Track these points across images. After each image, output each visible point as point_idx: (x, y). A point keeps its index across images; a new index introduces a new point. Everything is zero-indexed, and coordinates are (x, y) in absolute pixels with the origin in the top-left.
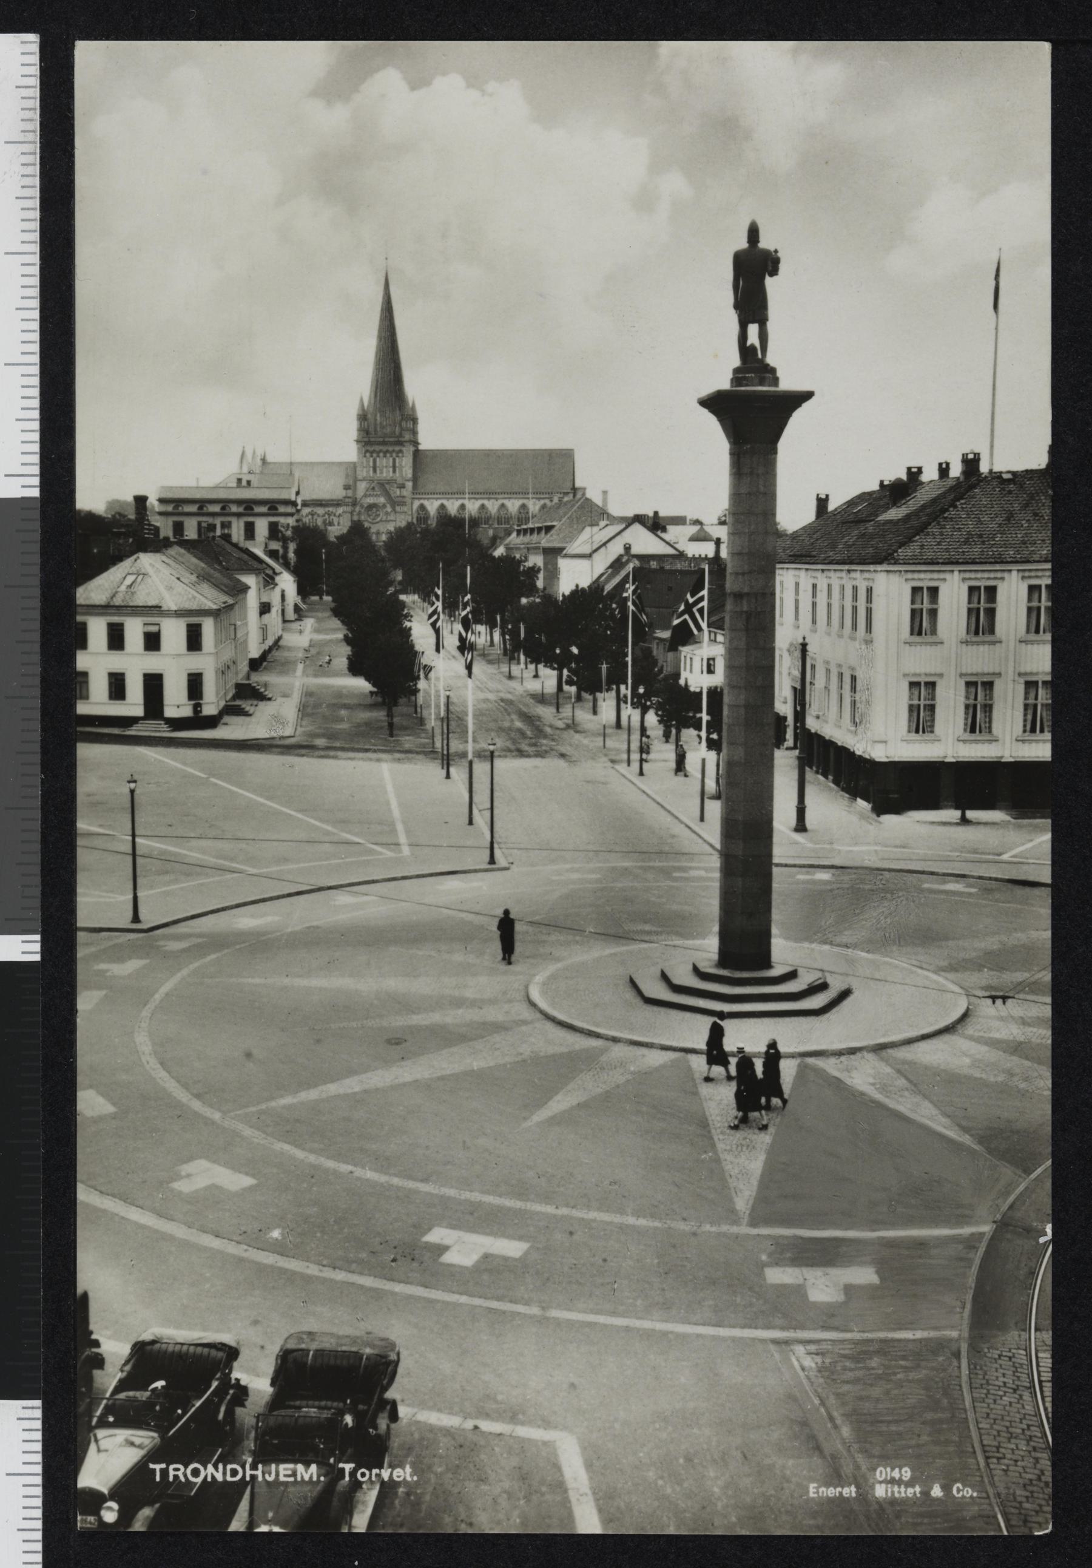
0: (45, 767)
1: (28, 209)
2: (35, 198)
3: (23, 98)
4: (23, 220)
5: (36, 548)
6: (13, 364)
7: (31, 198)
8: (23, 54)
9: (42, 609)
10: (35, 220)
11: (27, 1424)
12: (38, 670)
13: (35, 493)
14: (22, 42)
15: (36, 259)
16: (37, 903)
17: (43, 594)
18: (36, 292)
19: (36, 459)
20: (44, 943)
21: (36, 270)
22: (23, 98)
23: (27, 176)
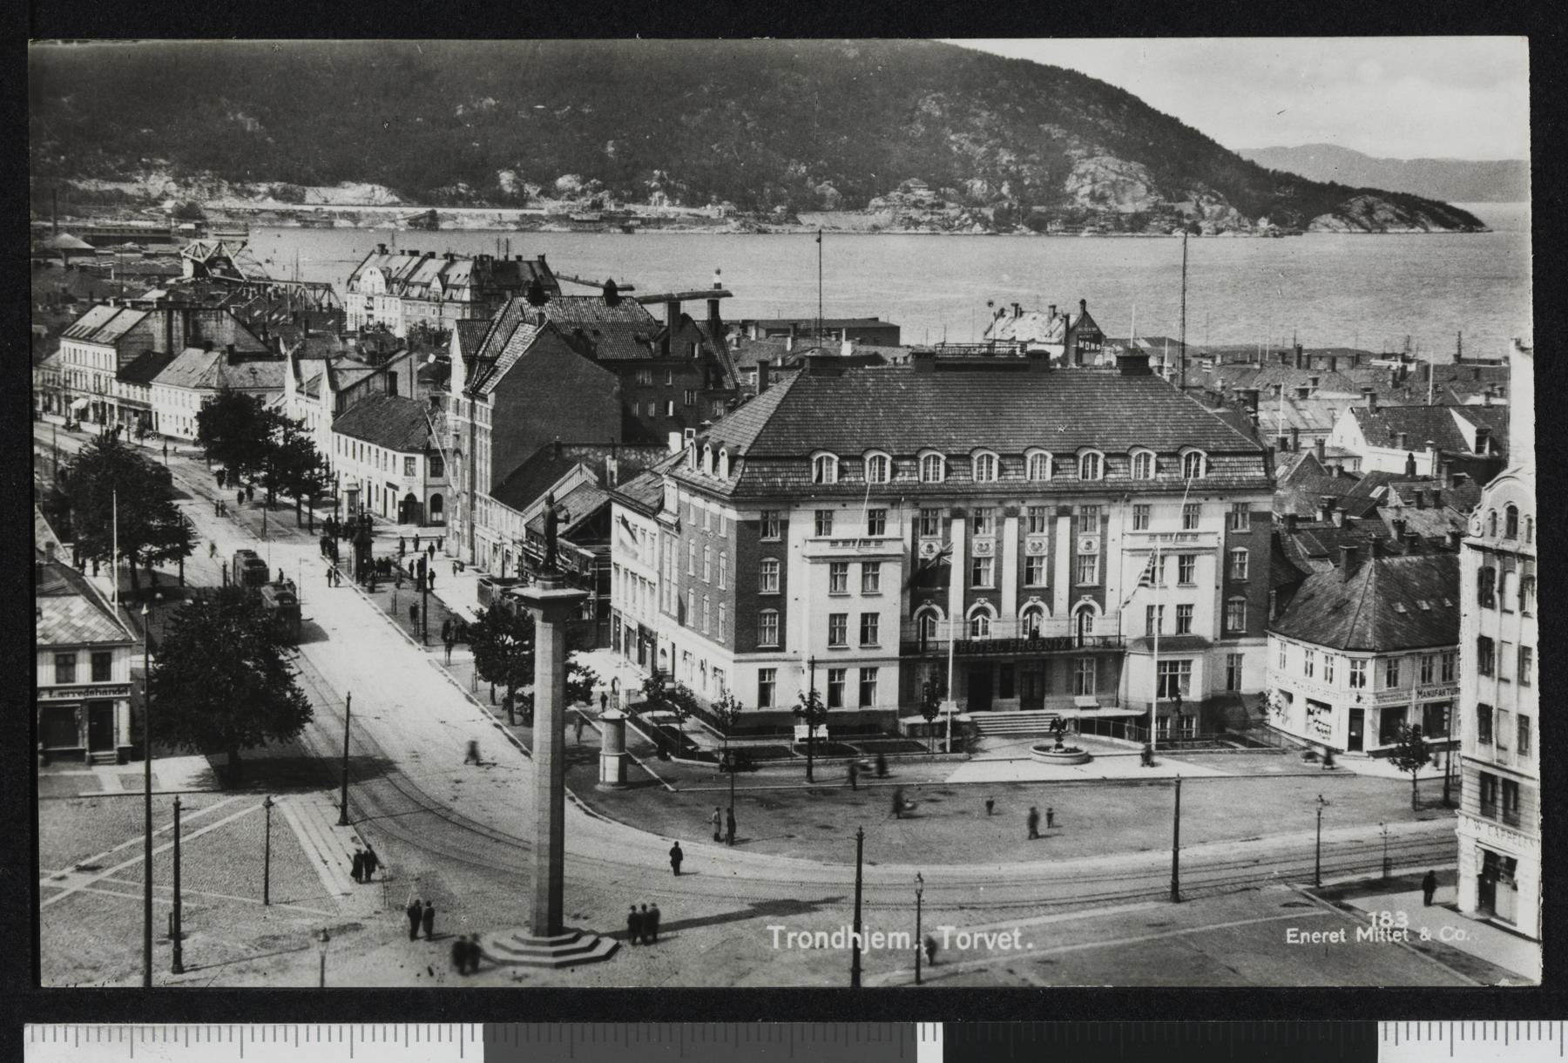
0: (751, 1018)
5: (533, 1026)
11: (1402, 1035)
13: (479, 1027)
15: (247, 1027)
16: (885, 1026)
17: (579, 1020)
18: (280, 1027)
19: (445, 1027)
21: (258, 1027)
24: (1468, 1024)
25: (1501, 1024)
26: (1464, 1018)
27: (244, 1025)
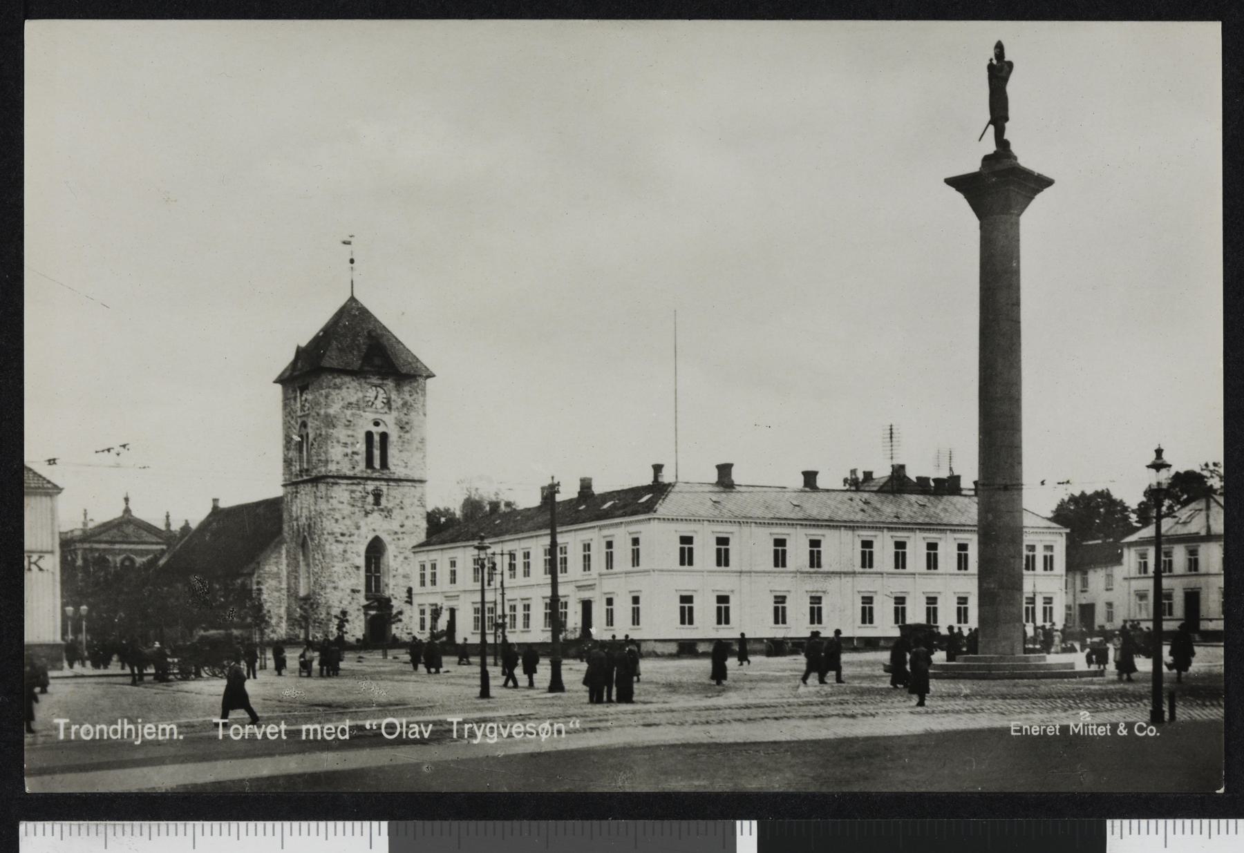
0: (602, 817)
1: (159, 830)
2: (150, 825)
3: (70, 835)
4: (168, 835)
5: (428, 824)
6: (282, 842)
7: (150, 828)
8: (35, 835)
10: (167, 825)
11: (1126, 831)
12: (526, 822)
13: (385, 824)
14: (26, 835)
15: (199, 824)
16: (711, 823)
18: (225, 824)
19: (357, 824)
20: (743, 818)
21: (207, 824)
22: (70, 835)
23: (132, 831)
24: (1179, 822)
25: (1205, 822)
26: (1175, 817)
27: (196, 822)
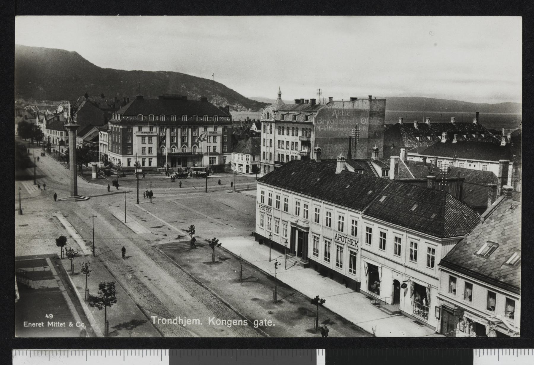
0: (261, 347)
5: (186, 350)
9: (207, 348)
11: (482, 354)
12: (227, 350)
13: (167, 351)
16: (306, 350)
17: (201, 348)
19: (156, 351)
24: (504, 350)
25: (515, 350)
